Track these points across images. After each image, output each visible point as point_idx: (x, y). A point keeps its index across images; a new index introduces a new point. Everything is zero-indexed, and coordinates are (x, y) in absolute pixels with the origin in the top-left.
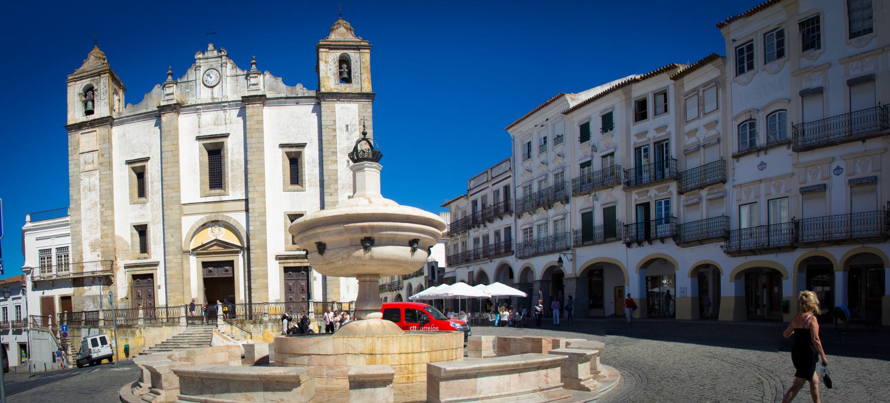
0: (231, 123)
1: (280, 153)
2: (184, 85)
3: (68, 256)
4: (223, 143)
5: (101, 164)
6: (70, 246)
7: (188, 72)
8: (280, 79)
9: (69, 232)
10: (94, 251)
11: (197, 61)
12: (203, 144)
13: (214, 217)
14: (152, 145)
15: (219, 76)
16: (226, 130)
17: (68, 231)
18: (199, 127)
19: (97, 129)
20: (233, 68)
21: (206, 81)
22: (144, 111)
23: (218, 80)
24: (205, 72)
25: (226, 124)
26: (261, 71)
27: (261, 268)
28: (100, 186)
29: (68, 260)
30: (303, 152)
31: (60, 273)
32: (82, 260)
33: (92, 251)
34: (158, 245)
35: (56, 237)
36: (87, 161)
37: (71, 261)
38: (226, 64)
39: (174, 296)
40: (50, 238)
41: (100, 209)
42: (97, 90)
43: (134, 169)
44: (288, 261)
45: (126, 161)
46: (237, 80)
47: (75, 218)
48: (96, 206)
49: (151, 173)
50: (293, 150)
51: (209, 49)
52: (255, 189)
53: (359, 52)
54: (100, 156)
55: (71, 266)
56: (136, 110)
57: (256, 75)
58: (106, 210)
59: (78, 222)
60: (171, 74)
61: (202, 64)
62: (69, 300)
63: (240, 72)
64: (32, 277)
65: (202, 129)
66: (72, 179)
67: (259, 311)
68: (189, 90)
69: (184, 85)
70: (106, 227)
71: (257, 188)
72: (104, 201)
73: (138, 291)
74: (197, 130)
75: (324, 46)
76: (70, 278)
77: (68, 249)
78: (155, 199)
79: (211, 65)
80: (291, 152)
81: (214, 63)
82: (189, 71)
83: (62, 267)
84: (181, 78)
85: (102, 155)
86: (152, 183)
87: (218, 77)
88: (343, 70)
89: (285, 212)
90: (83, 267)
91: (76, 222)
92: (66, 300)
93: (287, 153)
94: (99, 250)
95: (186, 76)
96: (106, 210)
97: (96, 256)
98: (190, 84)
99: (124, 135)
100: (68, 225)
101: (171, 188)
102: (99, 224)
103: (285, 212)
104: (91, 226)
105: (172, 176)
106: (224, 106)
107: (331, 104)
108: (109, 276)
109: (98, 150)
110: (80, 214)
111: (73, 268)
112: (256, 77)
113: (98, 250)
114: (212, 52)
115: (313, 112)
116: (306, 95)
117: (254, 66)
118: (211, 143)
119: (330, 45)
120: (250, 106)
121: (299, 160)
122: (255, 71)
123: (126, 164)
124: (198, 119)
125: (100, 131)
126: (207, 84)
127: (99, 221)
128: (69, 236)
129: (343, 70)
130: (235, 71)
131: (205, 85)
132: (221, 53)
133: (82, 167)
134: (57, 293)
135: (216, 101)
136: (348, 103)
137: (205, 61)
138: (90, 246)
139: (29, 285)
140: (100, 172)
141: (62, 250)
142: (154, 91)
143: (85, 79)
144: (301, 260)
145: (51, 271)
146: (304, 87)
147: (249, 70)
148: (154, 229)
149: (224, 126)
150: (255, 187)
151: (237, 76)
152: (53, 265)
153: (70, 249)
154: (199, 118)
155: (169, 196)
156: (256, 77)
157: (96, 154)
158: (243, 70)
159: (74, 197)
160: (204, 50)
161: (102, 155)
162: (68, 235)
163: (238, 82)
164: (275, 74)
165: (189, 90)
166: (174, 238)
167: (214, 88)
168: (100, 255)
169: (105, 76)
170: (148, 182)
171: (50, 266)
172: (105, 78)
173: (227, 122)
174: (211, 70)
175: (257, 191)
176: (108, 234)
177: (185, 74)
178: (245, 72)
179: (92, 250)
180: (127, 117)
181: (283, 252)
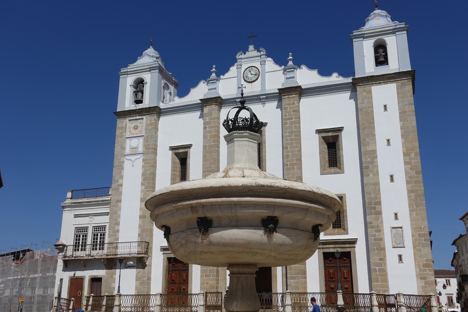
1: (316, 138)
3: (104, 235)
6: (107, 225)
9: (108, 211)
11: (238, 61)
17: (108, 211)
19: (144, 117)
21: (247, 77)
24: (246, 69)
26: (298, 64)
29: (104, 238)
30: (340, 136)
31: (94, 253)
32: (118, 239)
35: (94, 216)
37: (106, 241)
38: (265, 62)
40: (88, 216)
43: (177, 154)
44: (328, 246)
45: (170, 147)
51: (249, 50)
53: (395, 35)
55: (106, 246)
57: (293, 70)
61: (242, 63)
63: (277, 67)
64: (65, 256)
66: (116, 163)
67: (296, 301)
73: (173, 275)
75: (358, 37)
76: (103, 259)
77: (105, 228)
84: (223, 75)
88: (379, 55)
90: (116, 248)
92: (96, 281)
93: (323, 138)
100: (108, 204)
107: (367, 88)
108: (143, 257)
109: (143, 136)
111: (108, 248)
112: (292, 71)
114: (252, 52)
115: (351, 98)
119: (364, 34)
120: (286, 97)
121: (337, 144)
123: (169, 150)
125: (146, 119)
126: (247, 80)
128: (108, 215)
129: (379, 55)
131: (245, 81)
132: (260, 53)
136: (385, 84)
139: (60, 264)
141: (99, 229)
145: (85, 250)
146: (339, 75)
147: (286, 65)
156: (292, 71)
157: (141, 140)
158: (281, 66)
160: (245, 50)
162: (107, 214)
164: (311, 67)
171: (84, 245)
174: (251, 68)
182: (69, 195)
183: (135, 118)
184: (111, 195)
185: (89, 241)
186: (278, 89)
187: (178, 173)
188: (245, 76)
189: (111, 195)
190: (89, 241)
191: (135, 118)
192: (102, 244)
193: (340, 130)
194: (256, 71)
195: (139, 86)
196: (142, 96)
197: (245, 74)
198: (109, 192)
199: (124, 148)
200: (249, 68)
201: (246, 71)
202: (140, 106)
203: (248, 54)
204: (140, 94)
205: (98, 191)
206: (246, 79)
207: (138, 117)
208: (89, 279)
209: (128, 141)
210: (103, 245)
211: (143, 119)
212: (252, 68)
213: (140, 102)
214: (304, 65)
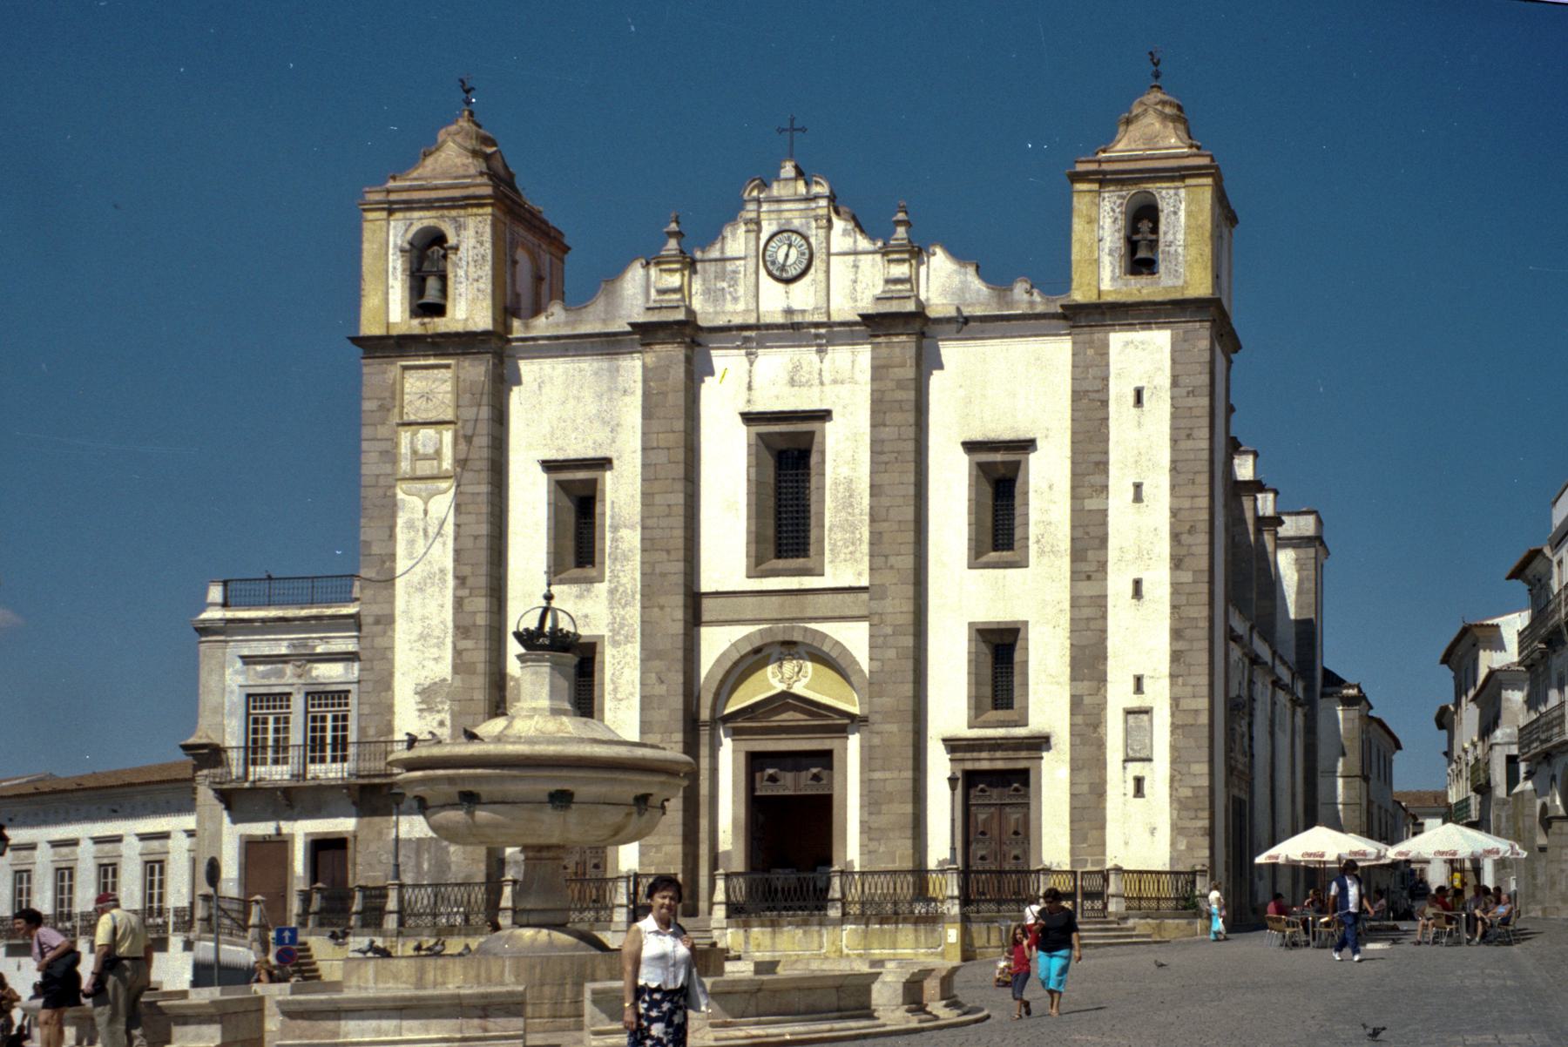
0: (835, 382)
2: (711, 267)
3: (345, 718)
4: (811, 434)
5: (461, 463)
7: (725, 234)
8: (971, 270)
10: (430, 710)
12: (759, 435)
13: (781, 631)
14: (618, 425)
15: (807, 251)
16: (821, 400)
17: (351, 646)
18: (750, 388)
20: (845, 233)
21: (773, 263)
22: (597, 328)
23: (805, 262)
25: (822, 383)
27: (895, 774)
28: (457, 526)
29: (345, 728)
31: (315, 769)
33: (421, 710)
34: (624, 703)
36: (421, 450)
37: (352, 736)
39: (656, 846)
41: (455, 589)
42: (456, 249)
46: (856, 266)
47: (376, 609)
48: (443, 581)
49: (613, 503)
50: (998, 457)
52: (886, 562)
54: (461, 441)
55: (352, 750)
56: (573, 323)
58: (471, 595)
59: (387, 621)
60: (678, 235)
62: (339, 853)
63: (863, 243)
65: (756, 394)
68: (725, 285)
69: (713, 269)
70: (469, 644)
71: (892, 560)
72: (467, 570)
74: (744, 395)
78: (621, 574)
79: (789, 221)
80: (995, 463)
81: (797, 214)
82: (727, 232)
83: (323, 750)
85: (469, 439)
86: (615, 528)
87: (803, 254)
89: (970, 624)
91: (377, 622)
94: (446, 707)
95: (718, 246)
96: (471, 595)
97: (435, 724)
98: (730, 266)
99: (540, 387)
101: (662, 550)
102: (450, 631)
103: (970, 624)
104: (423, 637)
105: (668, 516)
106: (817, 336)
110: (391, 600)
113: (440, 707)
116: (1040, 309)
117: (901, 232)
118: (781, 434)
122: (901, 245)
124: (747, 365)
126: (775, 272)
127: (450, 624)
130: (851, 240)
131: (770, 274)
133: (405, 466)
134: (301, 830)
135: (798, 319)
137: (775, 207)
138: (416, 693)
140: (458, 486)
142: (629, 275)
143: (421, 209)
144: (1011, 754)
148: (613, 656)
149: (816, 389)
150: (886, 557)
151: (856, 253)
152: (291, 742)
153: (353, 699)
154: (751, 364)
155: (657, 570)
159: (375, 550)
161: (469, 439)
163: (860, 271)
164: (959, 254)
165: (725, 285)
166: (664, 687)
167: (793, 287)
168: (448, 723)
169: (481, 211)
170: (603, 526)
172: (480, 218)
173: (824, 379)
174: (785, 235)
175: (892, 567)
176: (474, 663)
177: (715, 238)
178: (880, 244)
179: (424, 706)
180: (548, 338)
181: (962, 730)
182: (216, 593)
183: (422, 362)
184: (357, 599)
185: (296, 736)
186: (860, 315)
187: (570, 544)
188: (768, 258)
189: (357, 599)
190: (296, 736)
191: (422, 362)
192: (341, 744)
193: (1027, 445)
194: (802, 246)
195: (429, 252)
196: (444, 291)
197: (768, 253)
198: (351, 592)
199: (391, 456)
200: (780, 236)
201: (772, 244)
202: (440, 325)
203: (777, 190)
204: (432, 284)
205: (315, 584)
206: (771, 268)
207: (432, 361)
208: (306, 843)
209: (405, 437)
210: (344, 749)
211: (447, 367)
212: (790, 234)
213: (438, 310)
214: (941, 246)
